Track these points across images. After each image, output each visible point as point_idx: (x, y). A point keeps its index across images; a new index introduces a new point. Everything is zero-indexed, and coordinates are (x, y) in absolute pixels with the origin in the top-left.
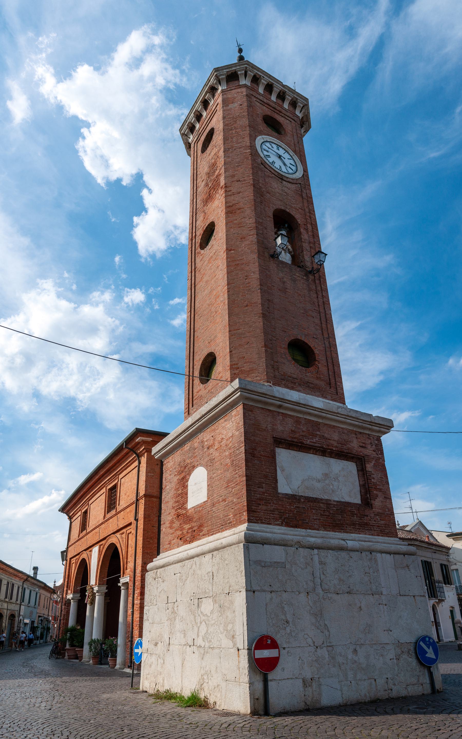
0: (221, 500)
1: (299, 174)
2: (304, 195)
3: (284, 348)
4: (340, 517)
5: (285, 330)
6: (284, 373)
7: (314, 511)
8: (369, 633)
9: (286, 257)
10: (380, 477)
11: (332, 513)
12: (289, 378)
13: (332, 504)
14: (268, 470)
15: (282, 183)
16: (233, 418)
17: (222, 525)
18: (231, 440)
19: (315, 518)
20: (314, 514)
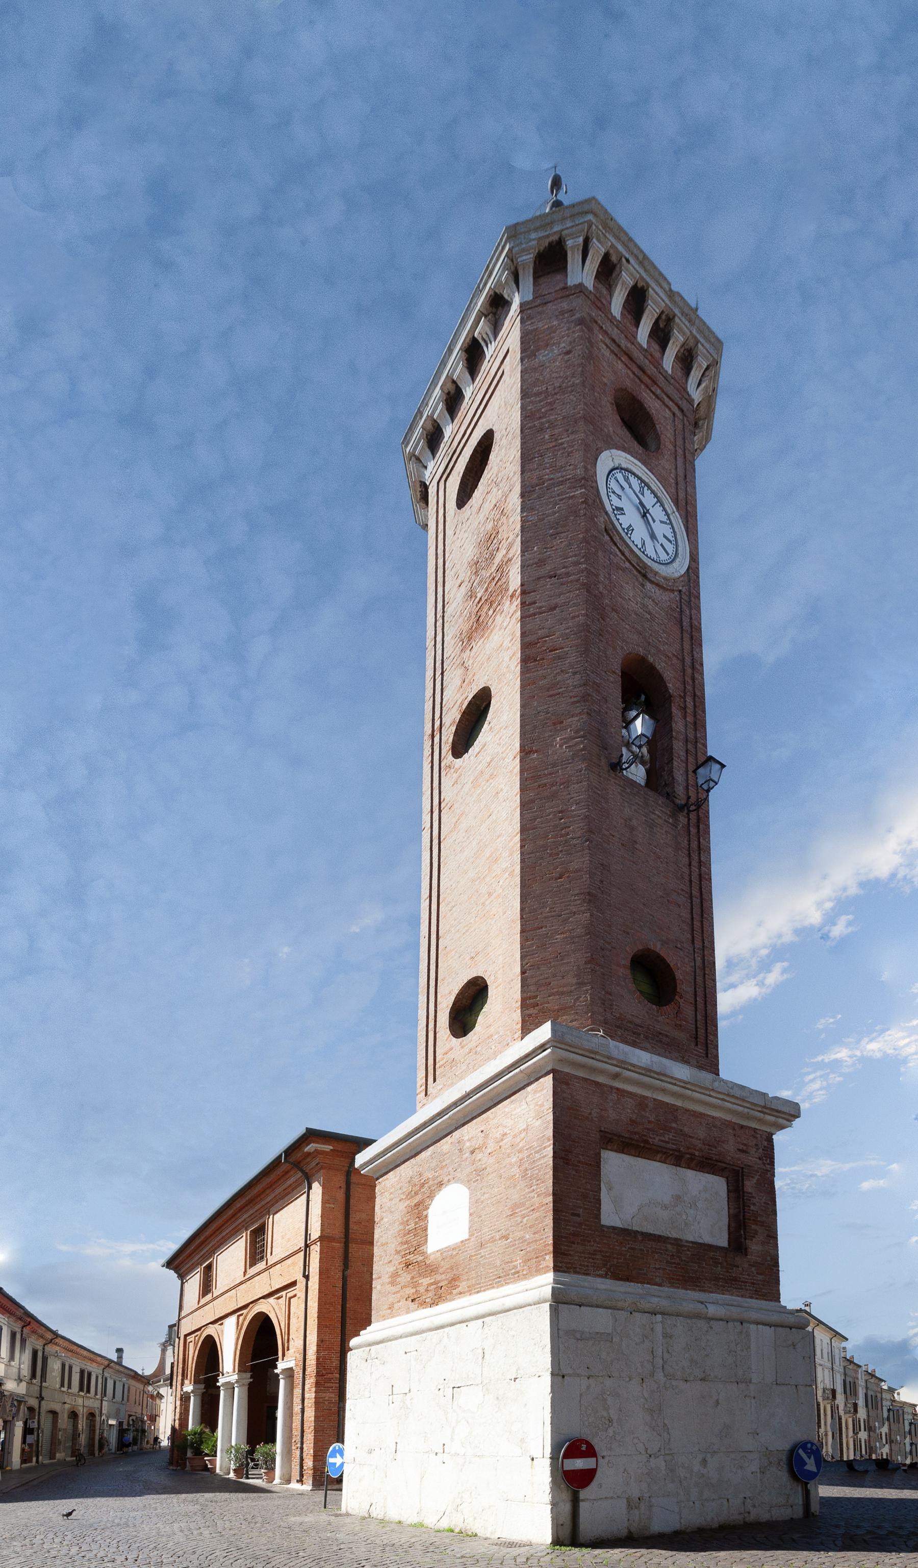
0: (498, 1237)
1: (680, 568)
2: (686, 623)
3: (624, 966)
4: (696, 1267)
5: (629, 931)
6: (621, 1014)
7: (656, 1255)
8: (726, 1437)
9: (638, 773)
10: (765, 1203)
11: (685, 1260)
12: (629, 1025)
13: (685, 1246)
16: (530, 1096)
17: (499, 1277)
18: (522, 1135)
19: (657, 1266)
20: (656, 1260)
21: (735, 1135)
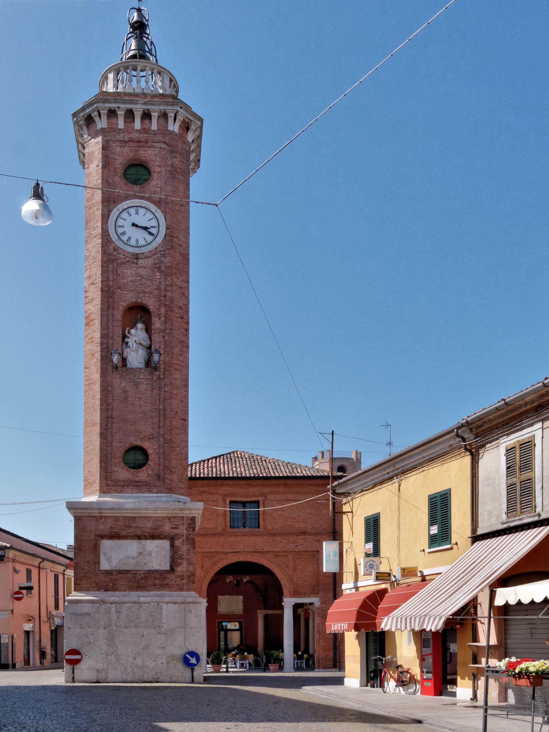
14: (90, 558)
15: (137, 263)
19: (123, 584)
21: (170, 522)
